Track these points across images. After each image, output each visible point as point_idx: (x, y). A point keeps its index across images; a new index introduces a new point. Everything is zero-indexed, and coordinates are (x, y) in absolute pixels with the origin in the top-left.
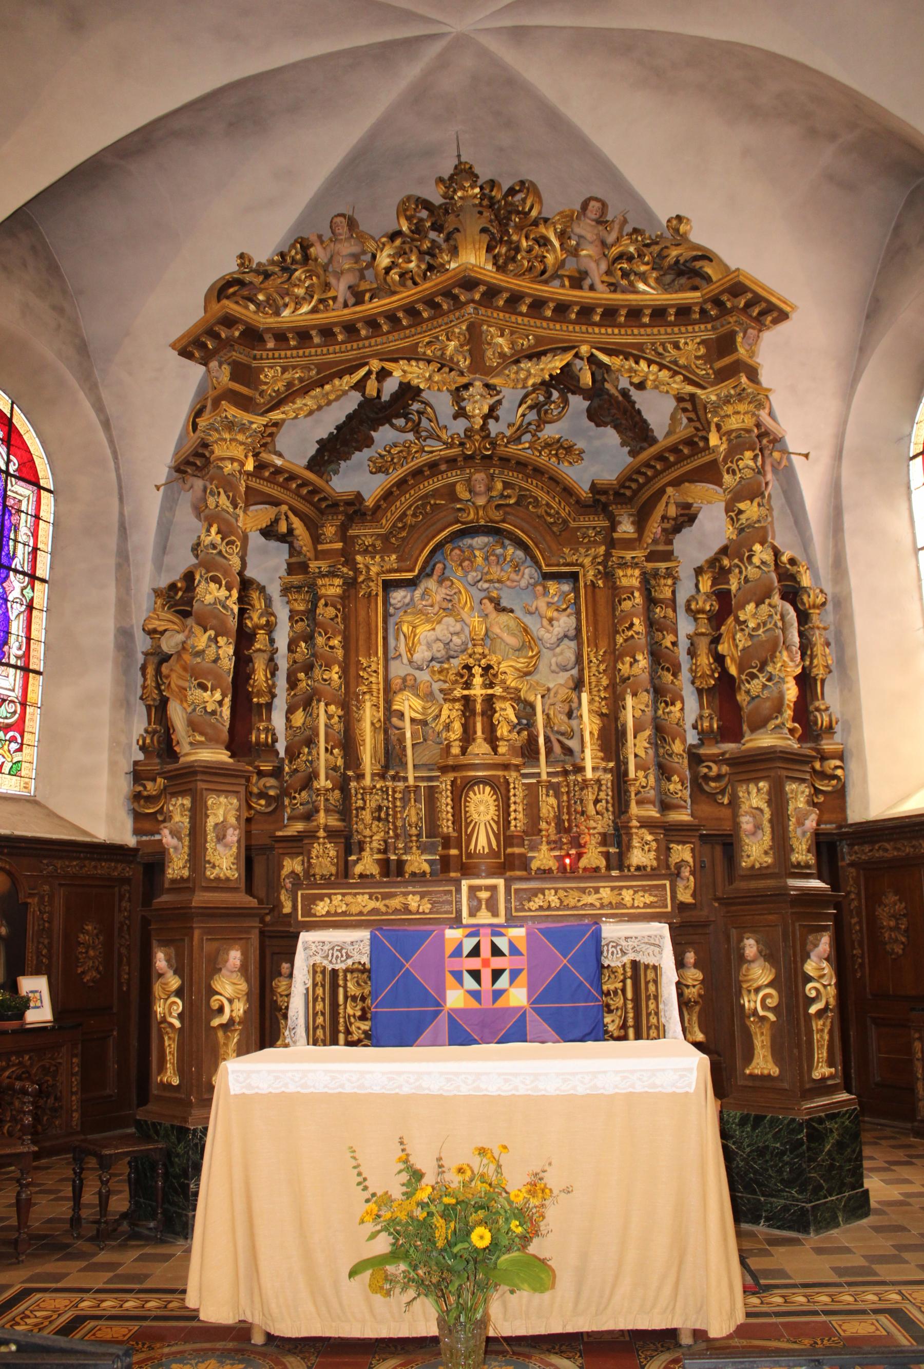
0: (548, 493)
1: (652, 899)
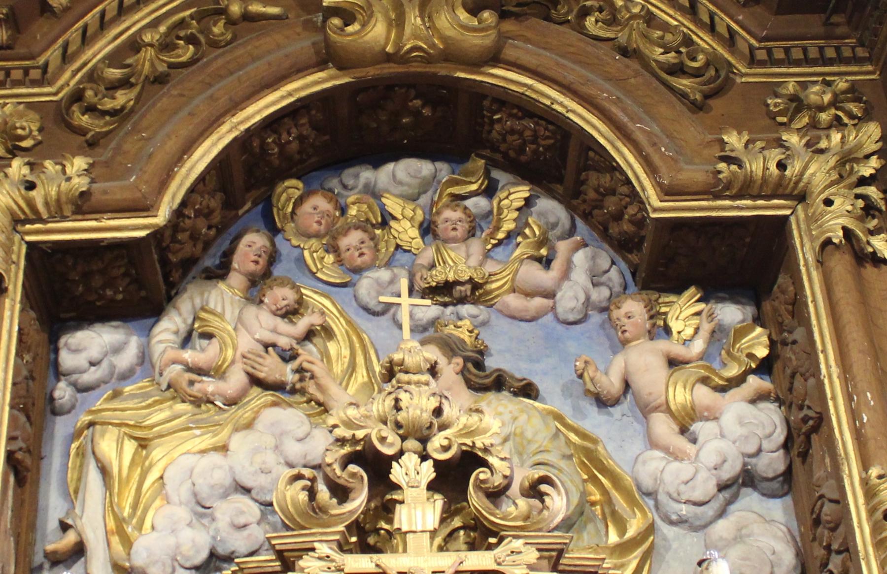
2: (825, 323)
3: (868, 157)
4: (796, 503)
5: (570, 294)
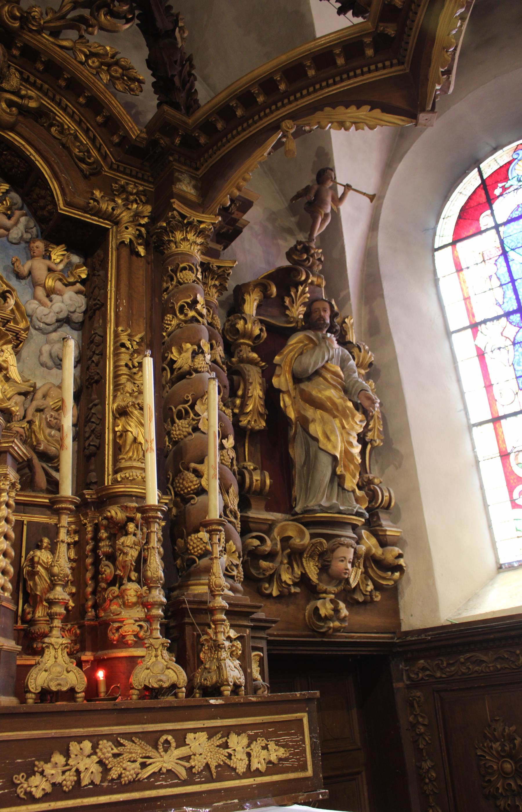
0: (79, 123)
1: (281, 752)
2: (114, 271)
3: (144, 217)
4: (83, 335)
5: (16, 232)
